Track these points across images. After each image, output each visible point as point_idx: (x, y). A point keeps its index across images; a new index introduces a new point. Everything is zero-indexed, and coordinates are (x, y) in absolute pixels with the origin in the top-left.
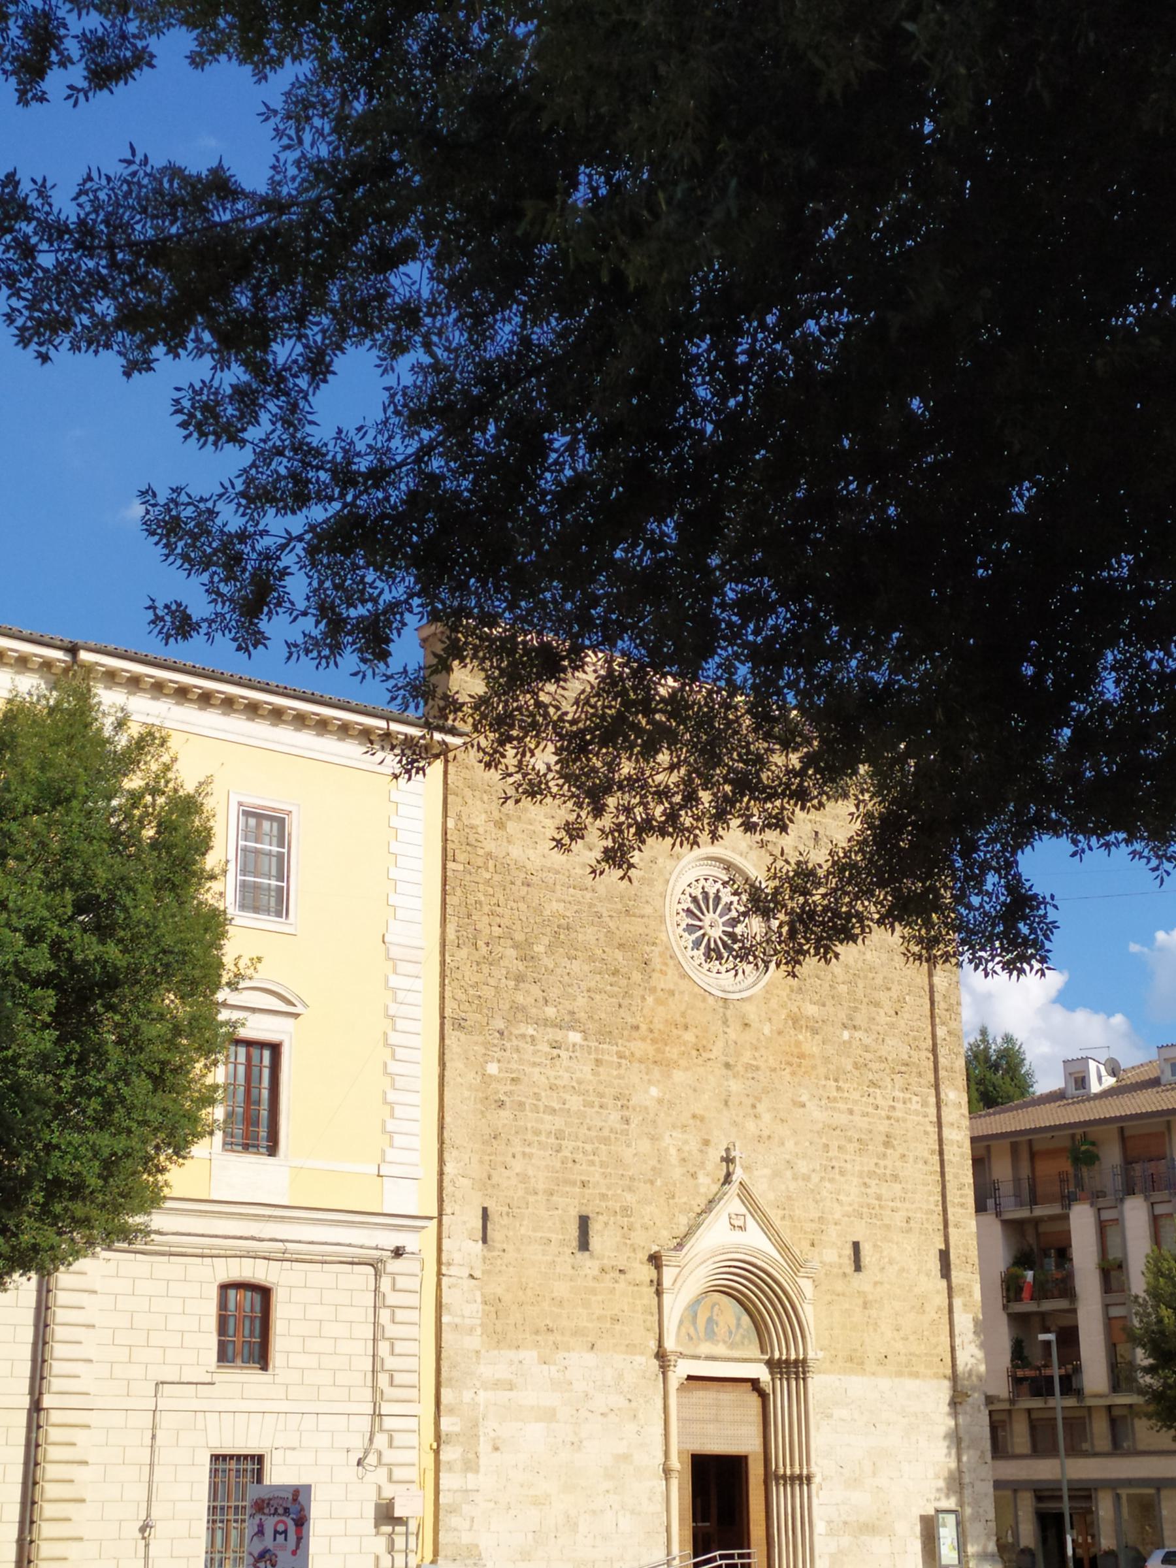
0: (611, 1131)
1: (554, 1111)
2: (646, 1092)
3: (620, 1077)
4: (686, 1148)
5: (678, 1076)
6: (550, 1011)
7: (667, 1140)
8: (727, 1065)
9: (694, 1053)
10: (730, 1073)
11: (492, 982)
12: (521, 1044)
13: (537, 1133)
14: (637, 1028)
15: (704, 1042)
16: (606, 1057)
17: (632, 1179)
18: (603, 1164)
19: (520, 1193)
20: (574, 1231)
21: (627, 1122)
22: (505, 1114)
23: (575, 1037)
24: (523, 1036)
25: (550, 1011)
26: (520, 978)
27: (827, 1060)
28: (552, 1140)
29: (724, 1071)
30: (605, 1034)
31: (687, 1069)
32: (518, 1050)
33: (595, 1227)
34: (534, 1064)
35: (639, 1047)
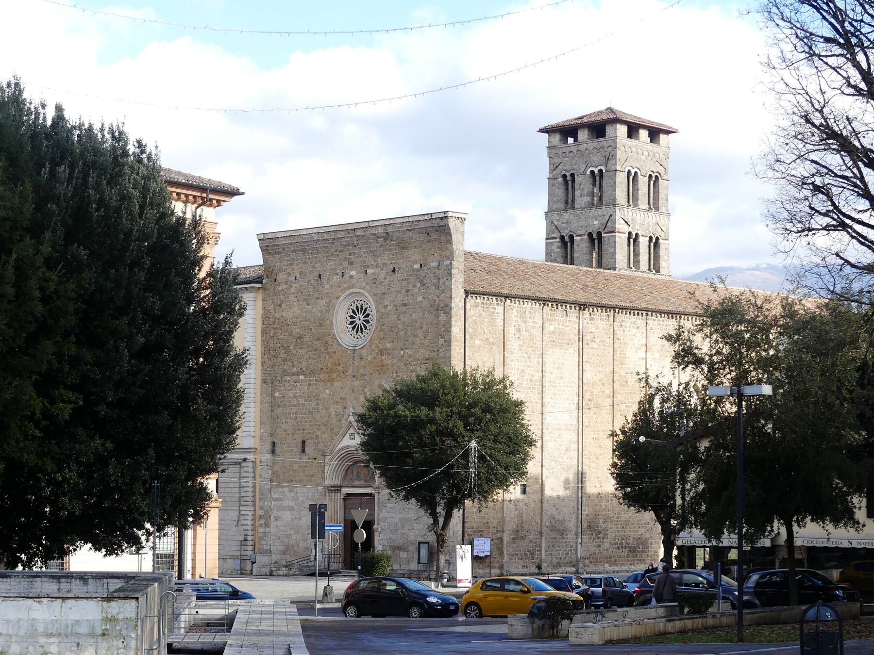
0: (313, 409)
1: (294, 405)
2: (325, 392)
3: (316, 389)
4: (338, 411)
5: (336, 384)
6: (294, 370)
7: (332, 409)
8: (354, 376)
9: (342, 374)
10: (355, 379)
11: (277, 364)
12: (286, 384)
13: (290, 414)
14: (323, 369)
15: (345, 369)
16: (312, 382)
17: (319, 425)
18: (310, 421)
19: (284, 435)
20: (300, 446)
21: (318, 404)
22: (281, 409)
23: (302, 377)
24: (286, 380)
25: (294, 370)
26: (285, 360)
27: (393, 365)
28: (294, 416)
29: (353, 379)
30: (312, 374)
31: (339, 381)
32: (284, 386)
33: (307, 444)
34: (289, 390)
35: (322, 376)
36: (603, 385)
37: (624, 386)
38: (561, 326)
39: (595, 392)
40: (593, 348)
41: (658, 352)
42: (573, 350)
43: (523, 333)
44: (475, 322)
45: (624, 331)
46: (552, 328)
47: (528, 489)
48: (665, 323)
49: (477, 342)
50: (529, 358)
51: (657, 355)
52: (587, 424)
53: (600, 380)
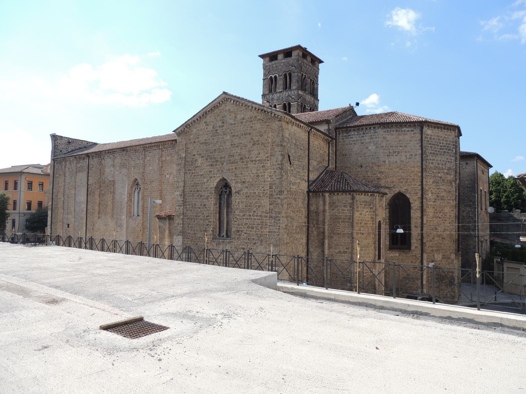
36: (96, 184)
37: (104, 184)
38: (82, 164)
39: (93, 187)
40: (93, 170)
41: (118, 167)
42: (85, 173)
43: (71, 169)
44: (57, 169)
45: (105, 161)
46: (79, 166)
47: (70, 226)
48: (122, 153)
49: (57, 175)
50: (72, 178)
51: (118, 168)
52: (89, 200)
53: (95, 182)
